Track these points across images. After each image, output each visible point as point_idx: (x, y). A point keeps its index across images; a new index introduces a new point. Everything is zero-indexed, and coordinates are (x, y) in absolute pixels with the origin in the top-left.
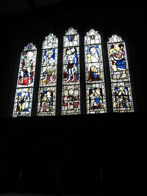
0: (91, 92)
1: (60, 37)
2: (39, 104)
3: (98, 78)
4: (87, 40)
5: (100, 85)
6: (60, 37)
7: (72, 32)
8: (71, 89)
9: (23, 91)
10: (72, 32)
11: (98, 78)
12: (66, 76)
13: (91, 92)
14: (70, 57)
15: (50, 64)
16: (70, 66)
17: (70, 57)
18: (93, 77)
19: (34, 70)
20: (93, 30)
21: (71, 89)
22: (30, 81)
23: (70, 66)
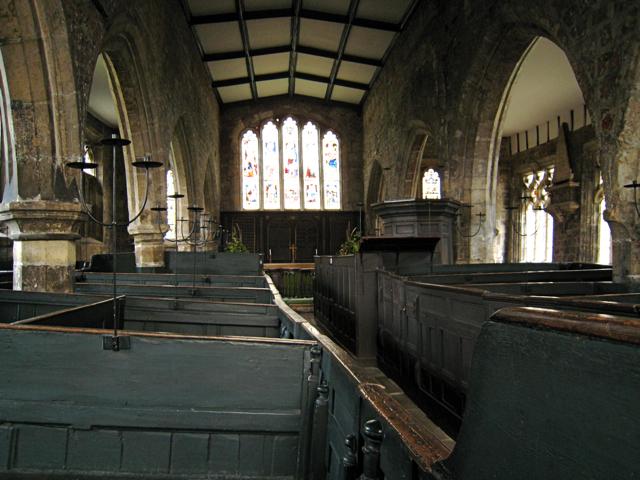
0: (308, 187)
1: (279, 126)
2: (265, 195)
3: (314, 176)
4: (304, 132)
5: (316, 181)
6: (279, 126)
7: (290, 123)
8: (291, 181)
9: (248, 183)
10: (290, 123)
11: (314, 176)
12: (287, 171)
13: (308, 187)
14: (290, 152)
15: (271, 159)
16: (290, 161)
17: (290, 152)
18: (309, 174)
19: (257, 162)
20: (309, 123)
21: (291, 181)
22: (254, 173)
23: (290, 161)
